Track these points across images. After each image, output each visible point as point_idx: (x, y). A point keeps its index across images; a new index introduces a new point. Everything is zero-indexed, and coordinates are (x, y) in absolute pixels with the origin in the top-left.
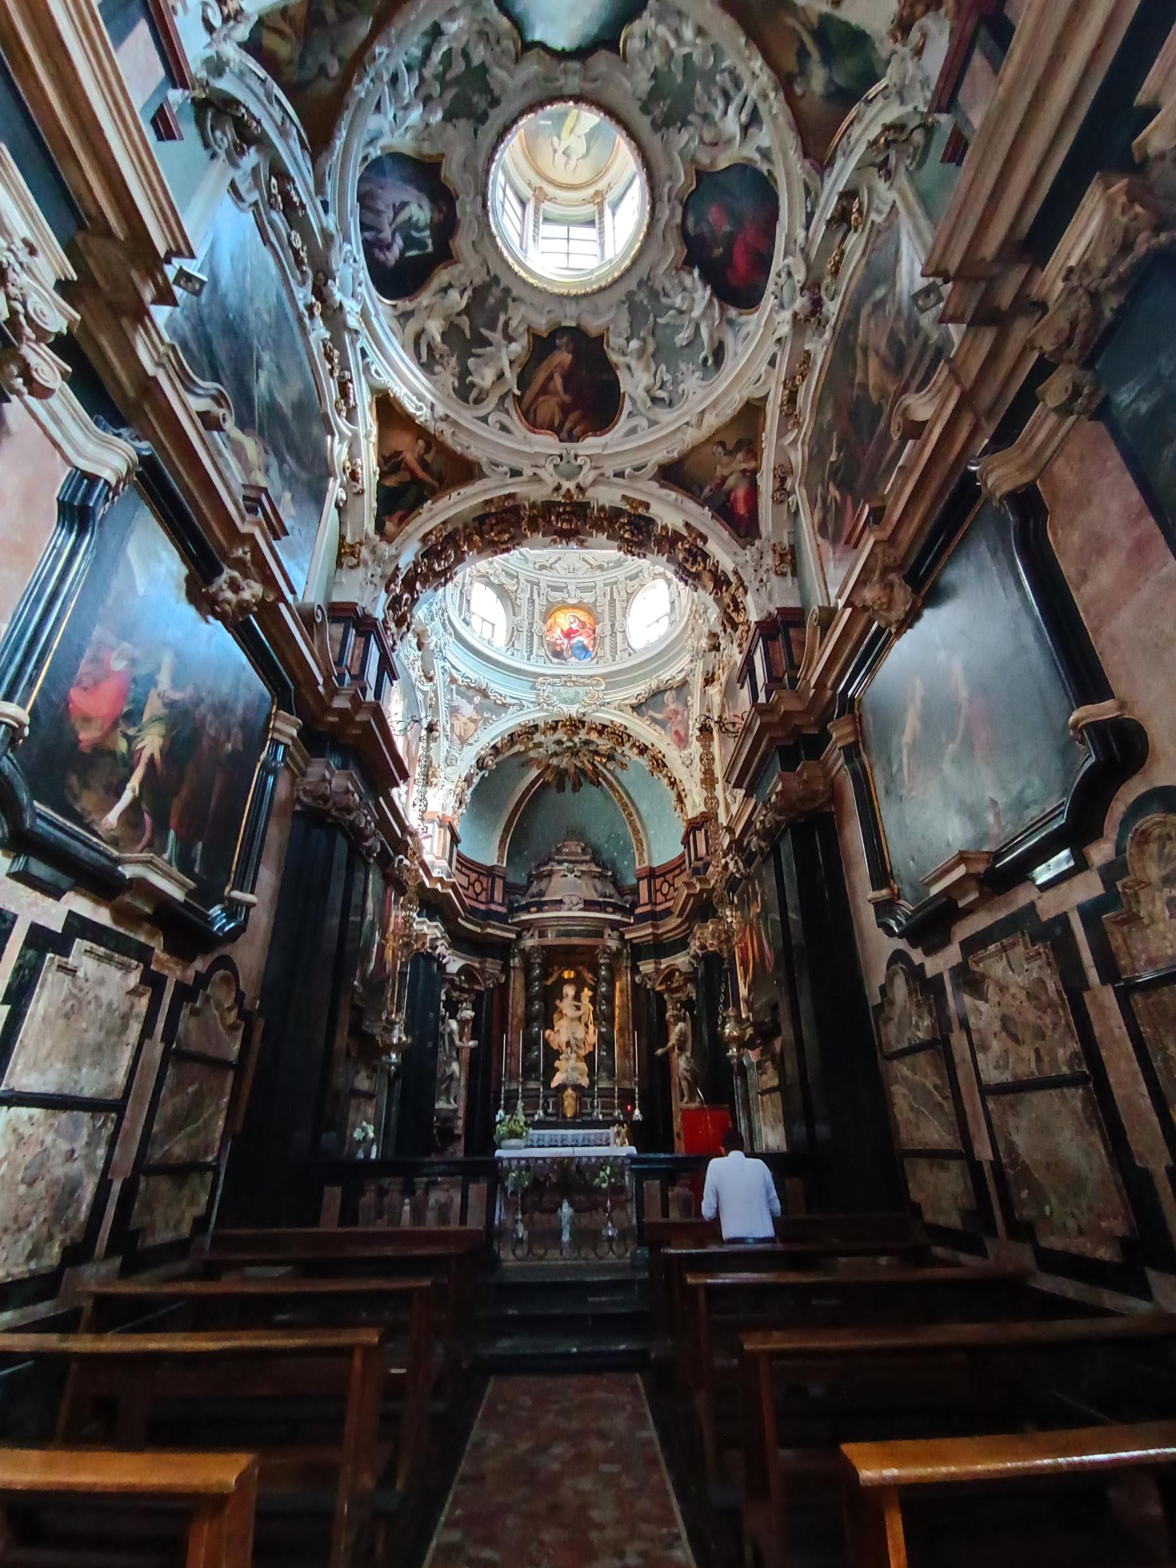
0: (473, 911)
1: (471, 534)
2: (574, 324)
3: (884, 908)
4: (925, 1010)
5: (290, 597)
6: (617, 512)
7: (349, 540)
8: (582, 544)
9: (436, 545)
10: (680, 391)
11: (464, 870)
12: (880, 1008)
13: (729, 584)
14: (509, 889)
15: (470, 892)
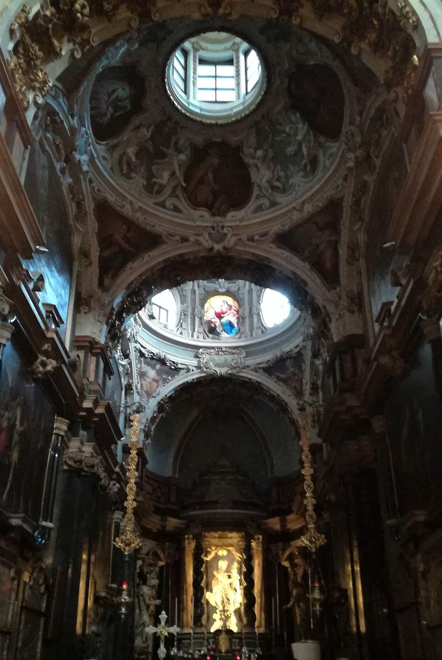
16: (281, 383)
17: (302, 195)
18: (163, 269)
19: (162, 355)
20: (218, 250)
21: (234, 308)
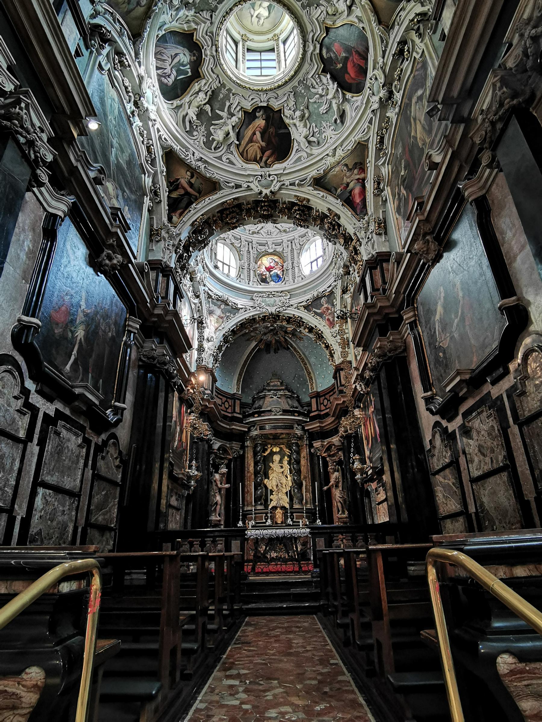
1: (216, 220)
2: (265, 105)
3: (428, 400)
4: (448, 448)
5: (133, 260)
6: (293, 204)
7: (155, 227)
8: (274, 222)
12: (430, 450)
14: (243, 405)
16: (318, 317)
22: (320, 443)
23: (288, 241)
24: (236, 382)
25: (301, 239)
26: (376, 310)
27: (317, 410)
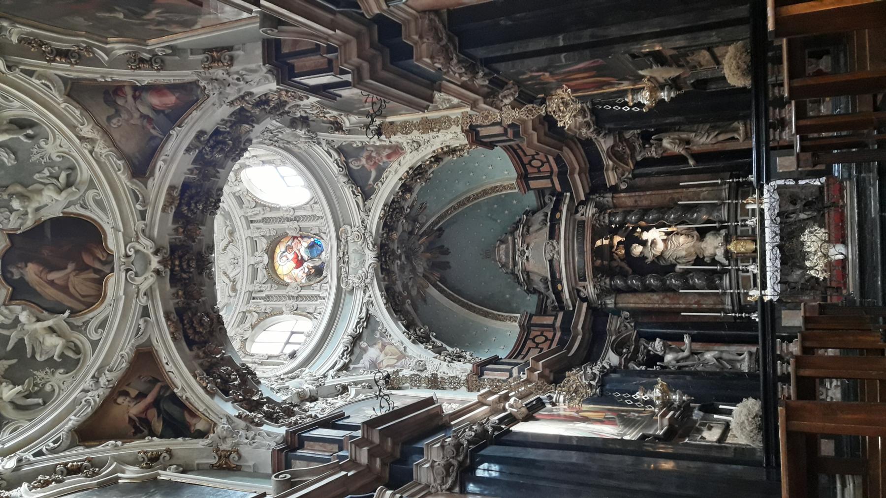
0: (562, 343)
1: (204, 352)
6: (178, 216)
8: (211, 248)
9: (216, 384)
10: (58, 160)
11: (524, 353)
13: (242, 109)
15: (545, 347)
16: (384, 175)
17: (70, 140)
18: (190, 343)
19: (347, 339)
20: (159, 262)
21: (289, 243)
22: (610, 173)
23: (249, 228)
24: (499, 322)
25: (246, 204)
26: (365, 65)
27: (550, 177)
